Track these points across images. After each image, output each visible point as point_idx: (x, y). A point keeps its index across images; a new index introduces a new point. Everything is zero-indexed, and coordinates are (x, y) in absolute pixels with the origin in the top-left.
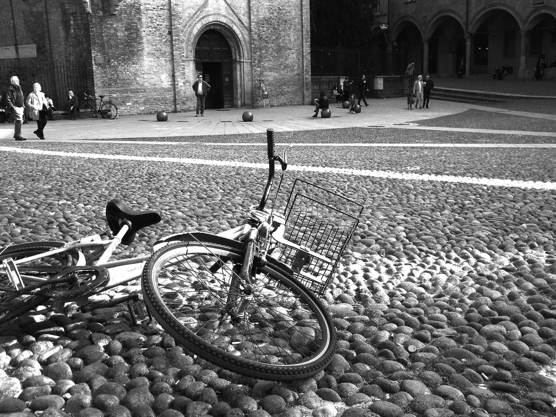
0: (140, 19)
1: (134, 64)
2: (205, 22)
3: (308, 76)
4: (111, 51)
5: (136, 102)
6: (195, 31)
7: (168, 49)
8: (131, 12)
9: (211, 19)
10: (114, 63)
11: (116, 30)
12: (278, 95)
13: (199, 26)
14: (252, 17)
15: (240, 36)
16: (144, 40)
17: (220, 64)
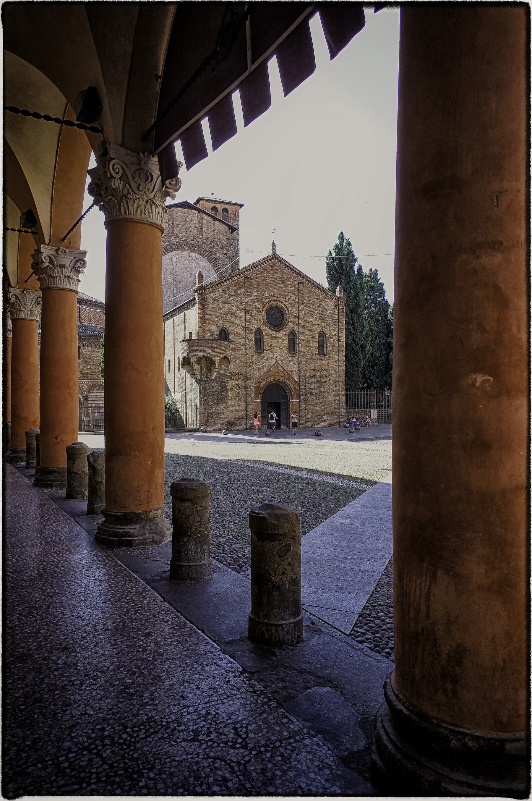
0: (228, 381)
1: (222, 404)
3: (343, 410)
6: (262, 385)
9: (272, 379)
10: (211, 403)
11: (213, 387)
13: (264, 383)
14: (301, 375)
15: (292, 387)
16: (229, 391)
17: (279, 403)
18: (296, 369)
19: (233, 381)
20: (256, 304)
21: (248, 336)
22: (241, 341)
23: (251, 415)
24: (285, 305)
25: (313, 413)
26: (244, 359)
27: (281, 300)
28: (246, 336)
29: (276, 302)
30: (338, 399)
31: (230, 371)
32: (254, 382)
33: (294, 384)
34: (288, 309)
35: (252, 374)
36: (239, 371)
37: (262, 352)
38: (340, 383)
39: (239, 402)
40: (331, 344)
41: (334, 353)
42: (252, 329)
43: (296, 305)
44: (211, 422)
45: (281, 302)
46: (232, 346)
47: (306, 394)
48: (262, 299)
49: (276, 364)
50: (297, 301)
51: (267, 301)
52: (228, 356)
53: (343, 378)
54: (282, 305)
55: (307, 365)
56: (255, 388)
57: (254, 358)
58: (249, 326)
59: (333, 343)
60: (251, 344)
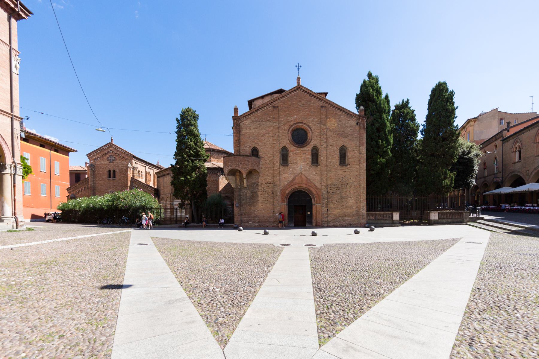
0: (258, 188)
1: (254, 206)
2: (293, 188)
3: (364, 212)
4: (243, 201)
5: (254, 222)
6: (287, 192)
7: (272, 200)
8: (254, 186)
9: (296, 186)
11: (246, 193)
12: (340, 221)
13: (289, 189)
14: (323, 183)
15: (315, 192)
16: (260, 196)
18: (318, 178)
19: (263, 188)
20: (282, 127)
21: (275, 153)
22: (269, 157)
23: (276, 215)
24: (308, 126)
25: (335, 215)
26: (272, 171)
27: (305, 122)
28: (273, 152)
29: (300, 124)
30: (359, 203)
31: (260, 181)
32: (281, 189)
33: (317, 191)
34: (311, 129)
35: (278, 183)
36: (268, 180)
37: (287, 165)
38: (361, 189)
39: (268, 205)
40: (352, 156)
41: (355, 163)
42: (278, 147)
43: (319, 125)
44: (245, 220)
45: (305, 124)
46: (262, 161)
47: (327, 199)
48: (288, 122)
49: (300, 174)
50: (320, 123)
51: (292, 124)
52: (256, 168)
53: (364, 184)
54: (306, 126)
55: (329, 174)
56: (281, 194)
57: (281, 170)
58: (276, 145)
59: (354, 155)
60: (277, 159)
